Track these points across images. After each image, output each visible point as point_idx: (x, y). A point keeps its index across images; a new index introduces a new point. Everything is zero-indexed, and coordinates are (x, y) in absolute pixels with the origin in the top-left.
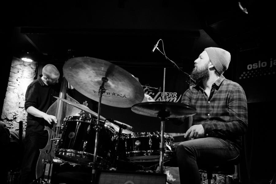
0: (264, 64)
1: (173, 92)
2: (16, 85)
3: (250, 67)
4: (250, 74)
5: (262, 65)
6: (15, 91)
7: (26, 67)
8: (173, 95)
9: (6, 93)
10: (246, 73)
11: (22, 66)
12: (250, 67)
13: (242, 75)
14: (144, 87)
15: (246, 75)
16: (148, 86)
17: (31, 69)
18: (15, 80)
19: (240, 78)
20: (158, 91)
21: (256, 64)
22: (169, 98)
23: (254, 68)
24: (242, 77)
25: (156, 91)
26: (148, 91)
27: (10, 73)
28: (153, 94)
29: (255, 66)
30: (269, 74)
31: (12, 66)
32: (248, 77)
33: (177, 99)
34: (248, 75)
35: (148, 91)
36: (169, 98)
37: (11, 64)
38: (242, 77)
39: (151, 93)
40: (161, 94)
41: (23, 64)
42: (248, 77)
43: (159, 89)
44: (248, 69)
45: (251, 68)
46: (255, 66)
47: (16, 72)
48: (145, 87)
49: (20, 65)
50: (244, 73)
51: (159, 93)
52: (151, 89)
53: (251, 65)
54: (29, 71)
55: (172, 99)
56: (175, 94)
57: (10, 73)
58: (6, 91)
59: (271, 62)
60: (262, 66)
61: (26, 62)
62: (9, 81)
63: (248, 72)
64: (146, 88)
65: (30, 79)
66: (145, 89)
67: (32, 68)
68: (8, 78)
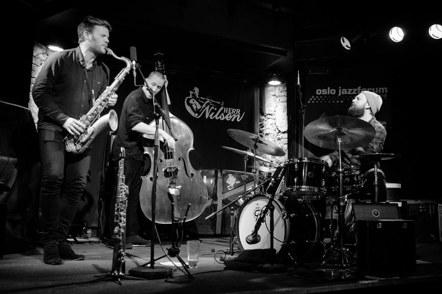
0: (333, 92)
1: (236, 109)
3: (319, 92)
4: (319, 99)
5: (333, 92)
8: (236, 112)
10: (315, 97)
12: (319, 92)
13: (311, 99)
14: (205, 101)
15: (315, 99)
16: (210, 99)
19: (309, 102)
20: (221, 107)
21: (326, 90)
22: (232, 114)
23: (323, 94)
24: (311, 101)
25: (219, 107)
26: (210, 105)
28: (216, 109)
29: (324, 92)
30: (338, 102)
31: (34, 55)
32: (317, 102)
33: (241, 116)
34: (317, 99)
35: (210, 105)
36: (232, 114)
38: (311, 101)
39: (213, 108)
40: (223, 110)
41: (46, 53)
42: (317, 102)
43: (221, 103)
44: (317, 93)
45: (320, 93)
46: (324, 92)
47: (39, 65)
48: (207, 100)
49: (42, 54)
50: (313, 97)
51: (222, 108)
52: (213, 103)
53: (320, 90)
55: (235, 116)
56: (238, 111)
57: (33, 65)
59: (340, 90)
60: (332, 93)
61: (52, 50)
62: (32, 77)
63: (317, 97)
66: (207, 102)
68: (31, 74)
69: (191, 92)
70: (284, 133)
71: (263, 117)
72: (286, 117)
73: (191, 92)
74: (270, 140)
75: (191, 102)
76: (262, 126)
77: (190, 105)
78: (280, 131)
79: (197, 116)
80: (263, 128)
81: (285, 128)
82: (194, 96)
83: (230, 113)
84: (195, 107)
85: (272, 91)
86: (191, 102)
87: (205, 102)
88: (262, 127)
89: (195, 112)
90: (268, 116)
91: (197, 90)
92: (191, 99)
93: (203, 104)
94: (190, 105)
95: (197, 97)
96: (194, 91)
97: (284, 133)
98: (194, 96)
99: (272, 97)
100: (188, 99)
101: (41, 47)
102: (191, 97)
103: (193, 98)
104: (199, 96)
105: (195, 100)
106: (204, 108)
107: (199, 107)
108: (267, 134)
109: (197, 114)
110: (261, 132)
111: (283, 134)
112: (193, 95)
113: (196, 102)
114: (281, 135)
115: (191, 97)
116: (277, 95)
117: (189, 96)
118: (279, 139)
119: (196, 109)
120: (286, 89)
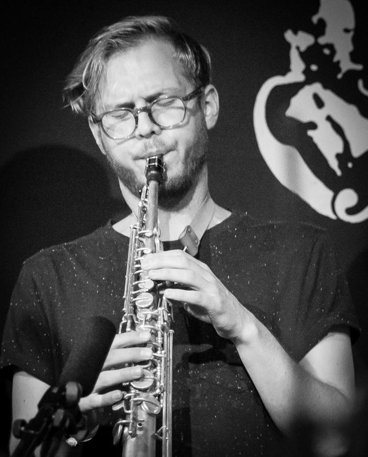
69: (299, 41)
73: (299, 41)
79: (351, 211)
89: (335, 184)
92: (294, 88)
95: (346, 65)
96: (319, 29)
100: (276, 90)
102: (296, 73)
103: (310, 78)
104: (354, 57)
105: (327, 96)
113: (334, 104)
115: (296, 73)
117: (285, 69)
119: (344, 156)
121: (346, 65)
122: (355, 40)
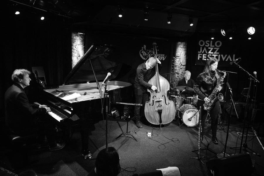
2: (75, 51)
6: (76, 55)
7: (78, 37)
9: (72, 58)
11: (77, 37)
14: (149, 51)
17: (81, 38)
18: (74, 48)
27: (71, 43)
37: (71, 37)
47: (74, 42)
54: (80, 40)
55: (162, 58)
56: (164, 55)
58: (72, 56)
64: (149, 52)
65: (82, 45)
66: (149, 52)
67: (82, 37)
69: (143, 48)
70: (184, 66)
71: (174, 58)
72: (185, 59)
73: (143, 48)
74: (177, 68)
75: (142, 52)
76: (174, 62)
77: (142, 54)
78: (182, 65)
80: (174, 63)
81: (184, 64)
82: (144, 50)
83: (159, 57)
84: (144, 55)
85: (180, 45)
86: (142, 52)
87: (148, 52)
88: (174, 62)
90: (177, 57)
91: (145, 46)
92: (141, 51)
93: (148, 53)
94: (142, 54)
95: (145, 50)
96: (144, 47)
97: (184, 66)
98: (144, 50)
99: (180, 48)
101: (75, 33)
106: (148, 55)
107: (146, 54)
108: (176, 66)
109: (145, 58)
110: (174, 64)
111: (183, 67)
112: (143, 49)
114: (182, 67)
116: (182, 47)
118: (181, 68)
120: (186, 45)
121: (145, 50)
122: (146, 48)
